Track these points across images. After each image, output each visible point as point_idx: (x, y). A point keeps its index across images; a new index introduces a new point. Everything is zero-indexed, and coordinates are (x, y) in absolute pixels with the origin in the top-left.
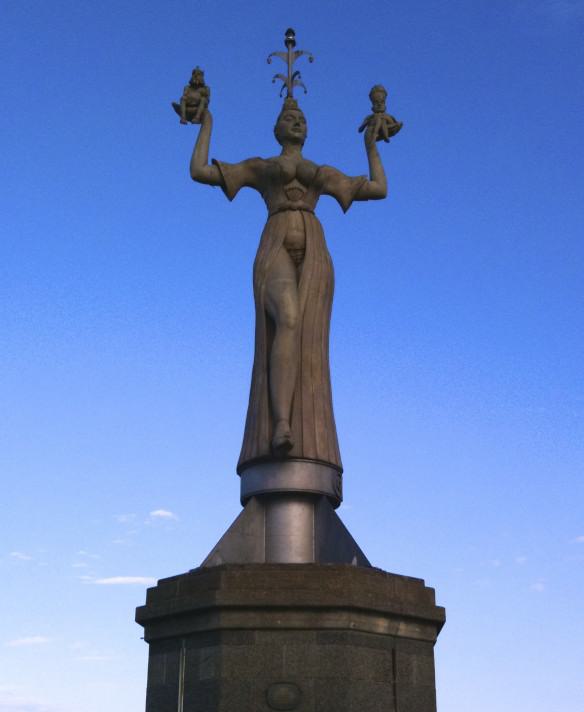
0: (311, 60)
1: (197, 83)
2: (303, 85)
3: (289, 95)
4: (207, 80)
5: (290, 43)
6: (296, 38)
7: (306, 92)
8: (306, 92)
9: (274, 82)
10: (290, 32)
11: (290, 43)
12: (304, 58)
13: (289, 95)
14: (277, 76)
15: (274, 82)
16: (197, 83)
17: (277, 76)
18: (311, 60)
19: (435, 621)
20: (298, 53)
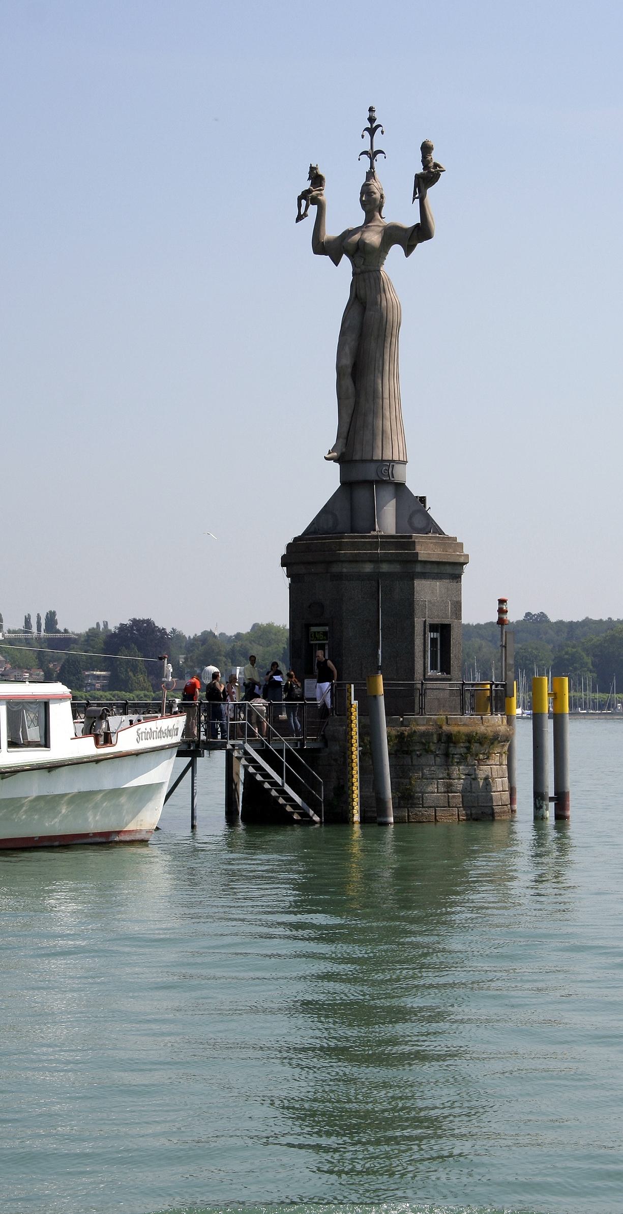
0: (382, 132)
2: (383, 153)
3: (372, 167)
4: (321, 171)
5: (371, 120)
6: (376, 115)
7: (385, 158)
8: (385, 158)
9: (359, 160)
10: (371, 110)
11: (371, 120)
12: (379, 130)
13: (372, 167)
14: (362, 154)
15: (359, 160)
17: (362, 154)
18: (382, 132)
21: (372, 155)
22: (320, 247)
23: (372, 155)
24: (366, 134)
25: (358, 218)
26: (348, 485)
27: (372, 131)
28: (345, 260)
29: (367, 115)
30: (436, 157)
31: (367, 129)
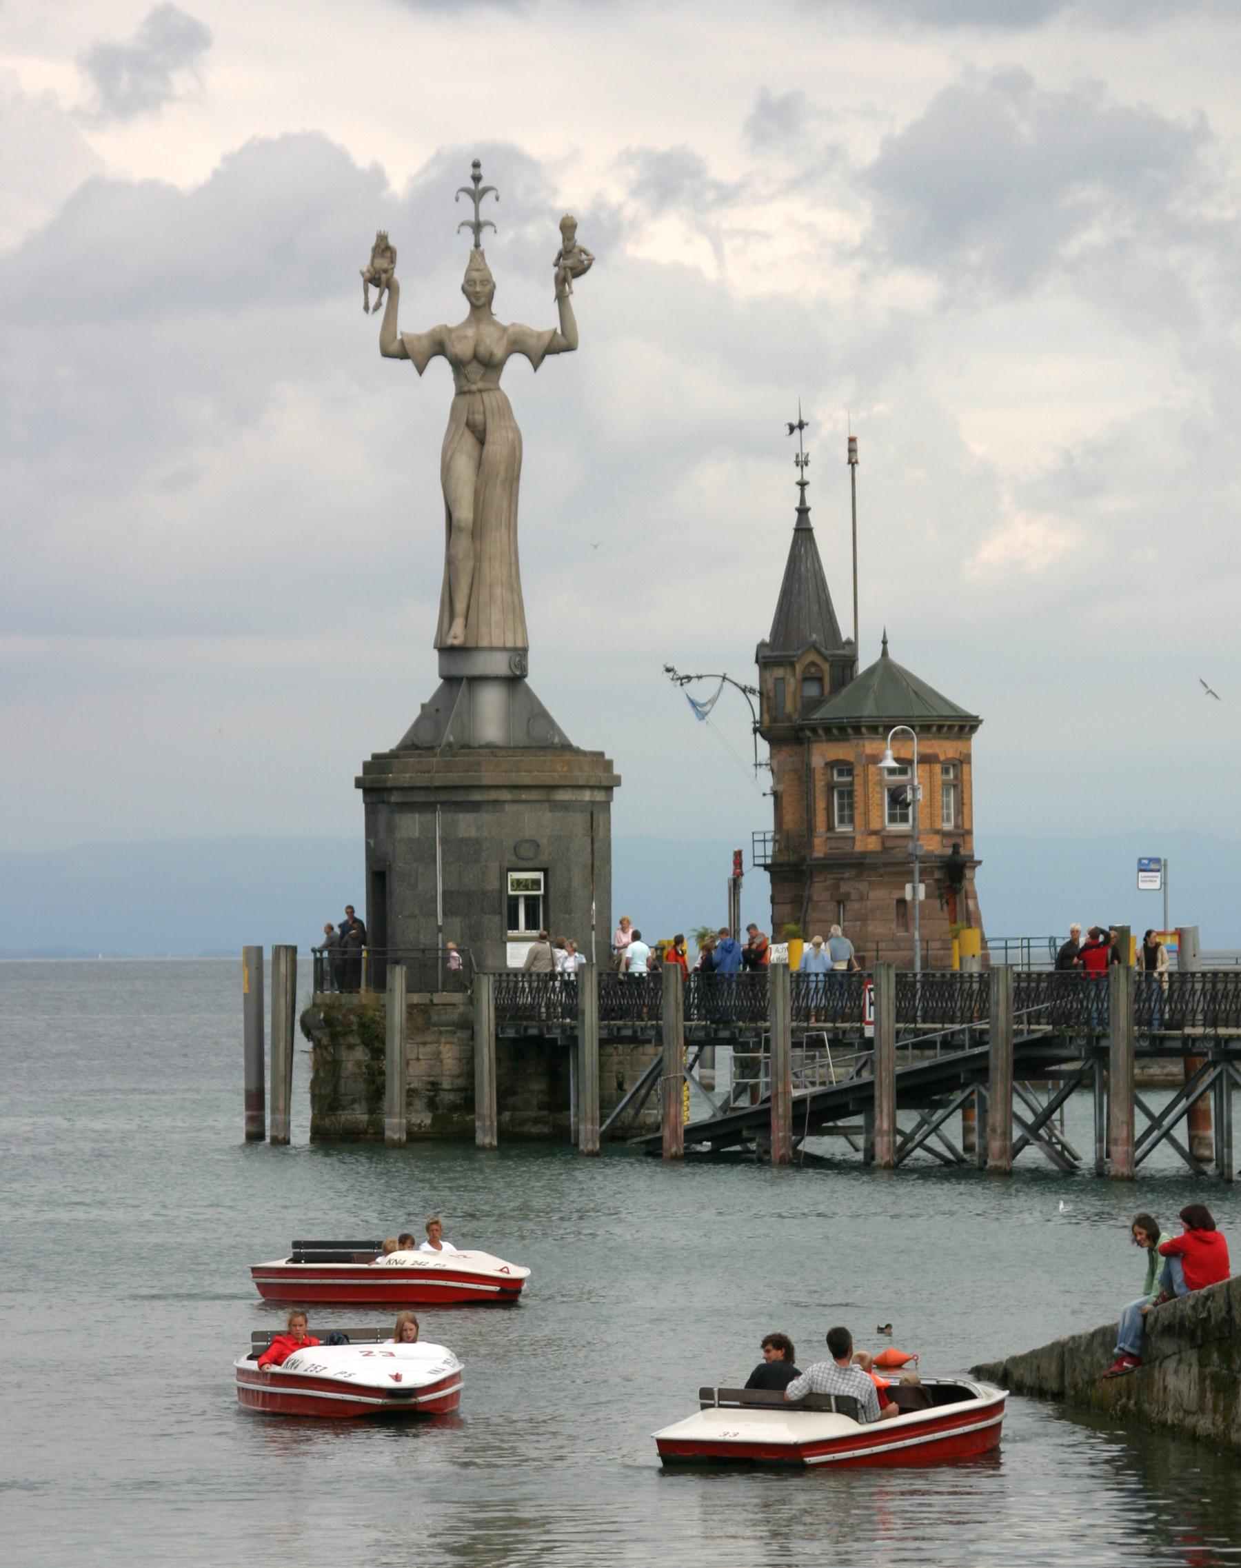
0: (497, 199)
1: (383, 249)
2: (492, 224)
3: (477, 245)
5: (477, 179)
6: (483, 171)
7: (495, 232)
8: (495, 232)
9: (459, 232)
10: (476, 165)
11: (477, 179)
13: (477, 245)
14: (463, 224)
15: (459, 232)
16: (383, 249)
17: (463, 224)
18: (497, 199)
19: (609, 785)
20: (486, 190)
21: (477, 227)
22: (393, 349)
23: (477, 227)
24: (466, 200)
25: (459, 310)
26: (450, 680)
27: (477, 196)
28: (440, 368)
29: (470, 171)
30: (581, 238)
31: (466, 190)
